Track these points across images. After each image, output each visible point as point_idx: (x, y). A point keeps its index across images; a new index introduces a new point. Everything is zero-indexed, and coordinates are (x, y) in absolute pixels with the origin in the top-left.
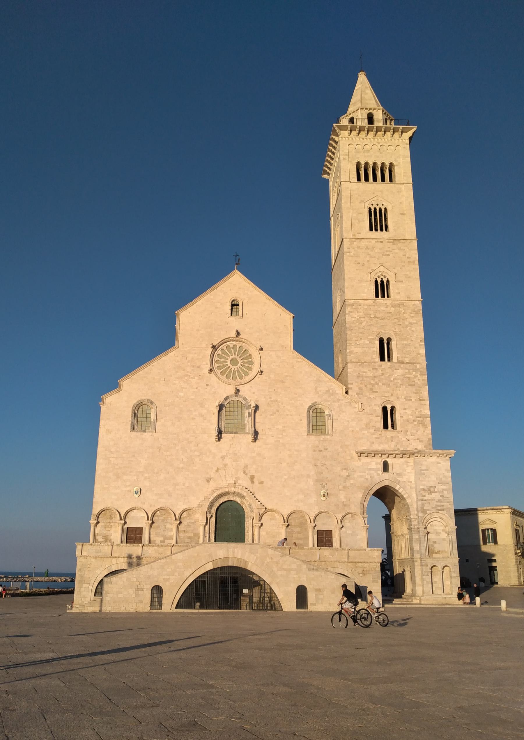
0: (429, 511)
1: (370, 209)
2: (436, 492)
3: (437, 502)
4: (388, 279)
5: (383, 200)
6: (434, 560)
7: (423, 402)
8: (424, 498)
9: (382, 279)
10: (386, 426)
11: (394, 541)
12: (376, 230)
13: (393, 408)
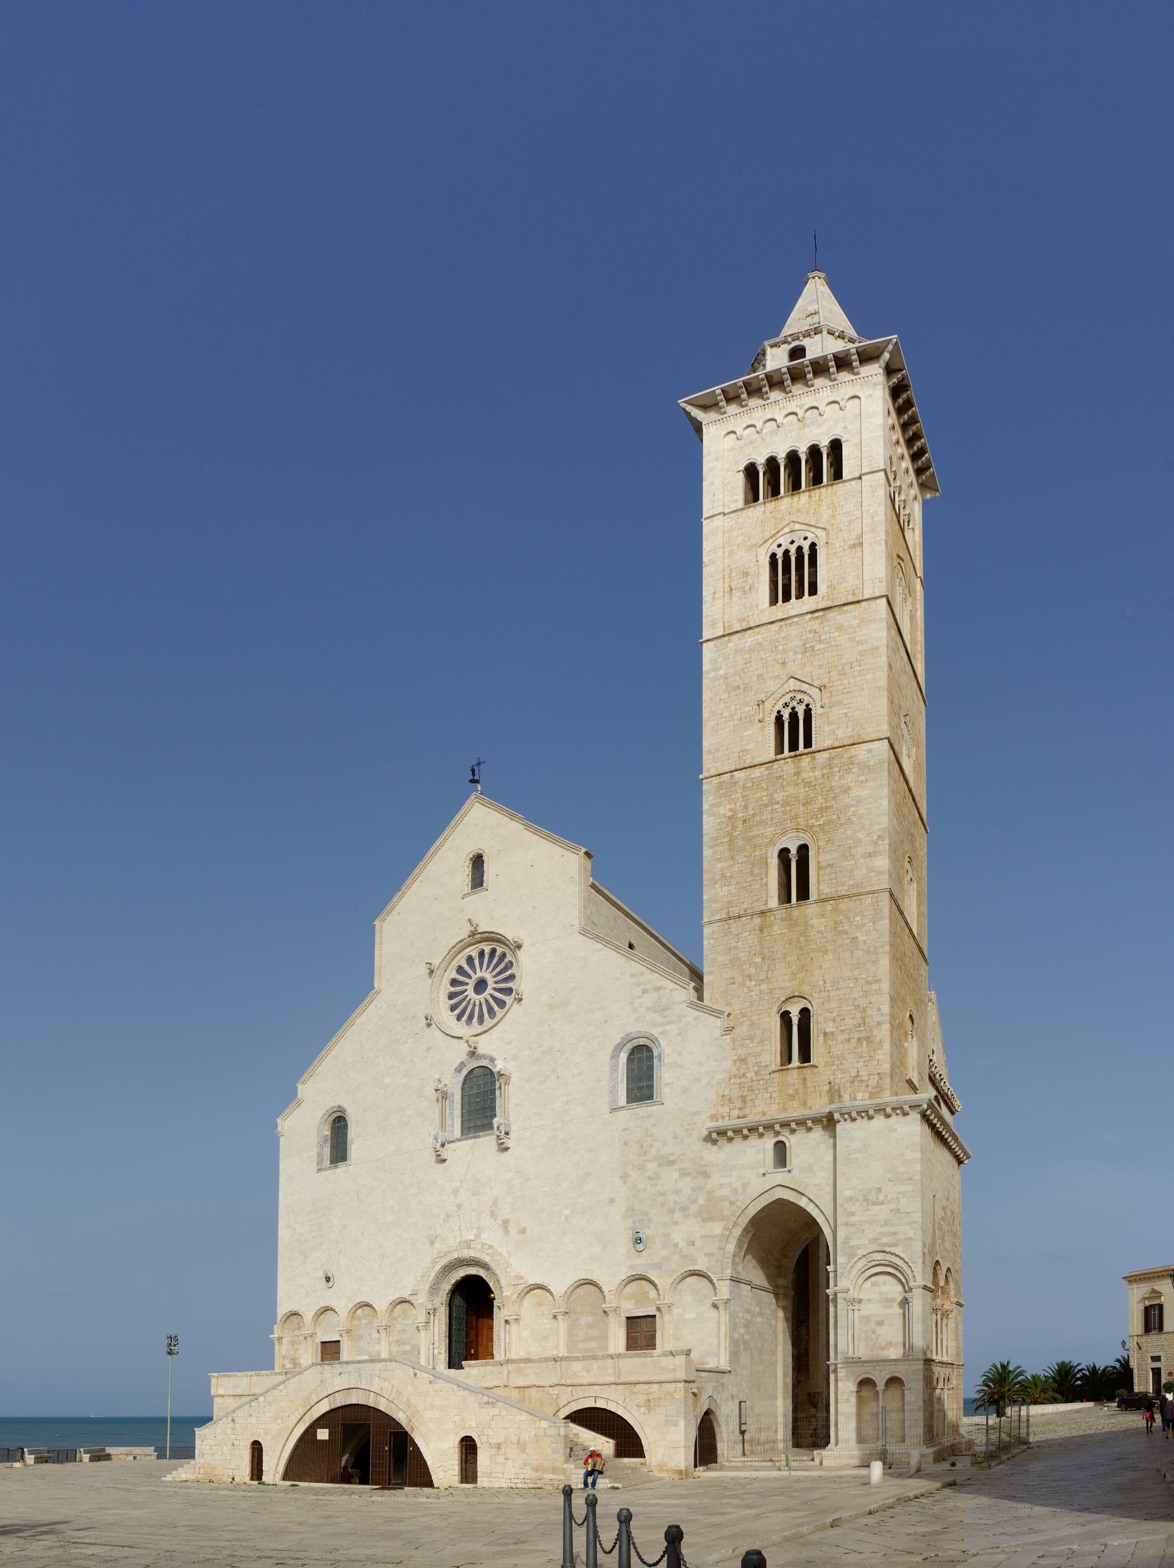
0: (861, 1248)
2: (882, 1203)
3: (882, 1226)
6: (865, 1365)
7: (875, 987)
8: (852, 1219)
9: (793, 708)
11: (784, 1331)
13: (805, 1013)
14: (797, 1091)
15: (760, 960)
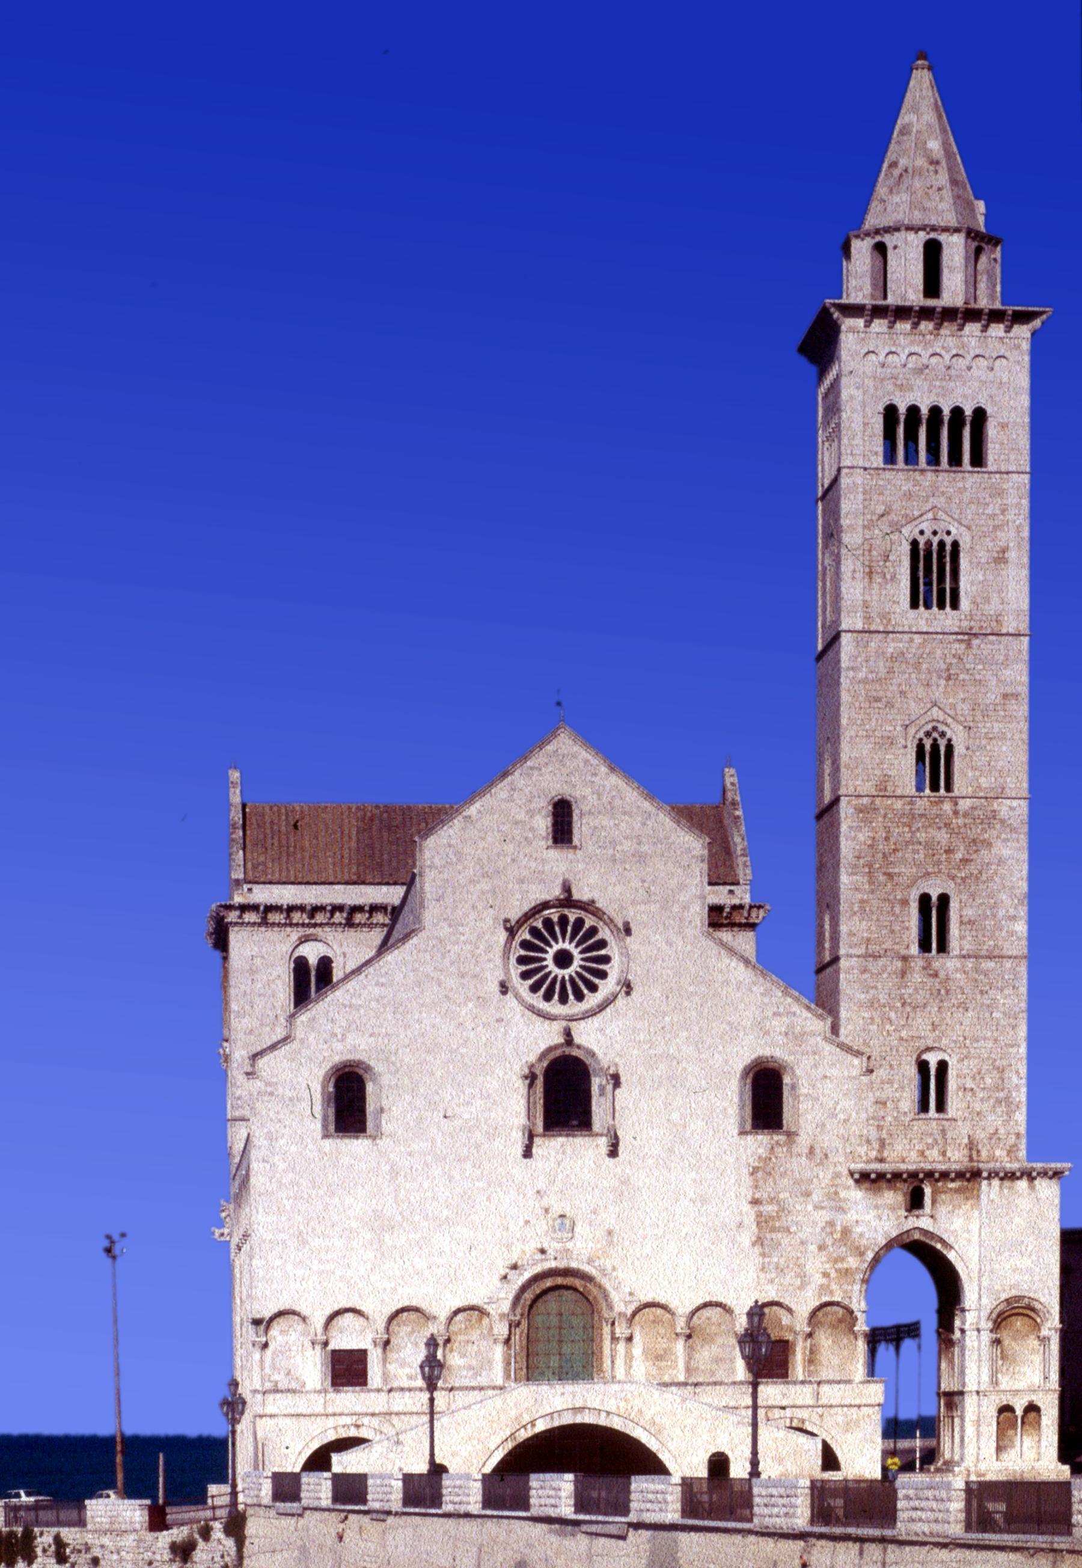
1: (915, 544)
4: (950, 740)
5: (949, 519)
7: (1013, 1050)
9: (935, 740)
10: (924, 1107)
12: (928, 606)
13: (943, 1066)
14: (936, 1140)
15: (899, 1005)
